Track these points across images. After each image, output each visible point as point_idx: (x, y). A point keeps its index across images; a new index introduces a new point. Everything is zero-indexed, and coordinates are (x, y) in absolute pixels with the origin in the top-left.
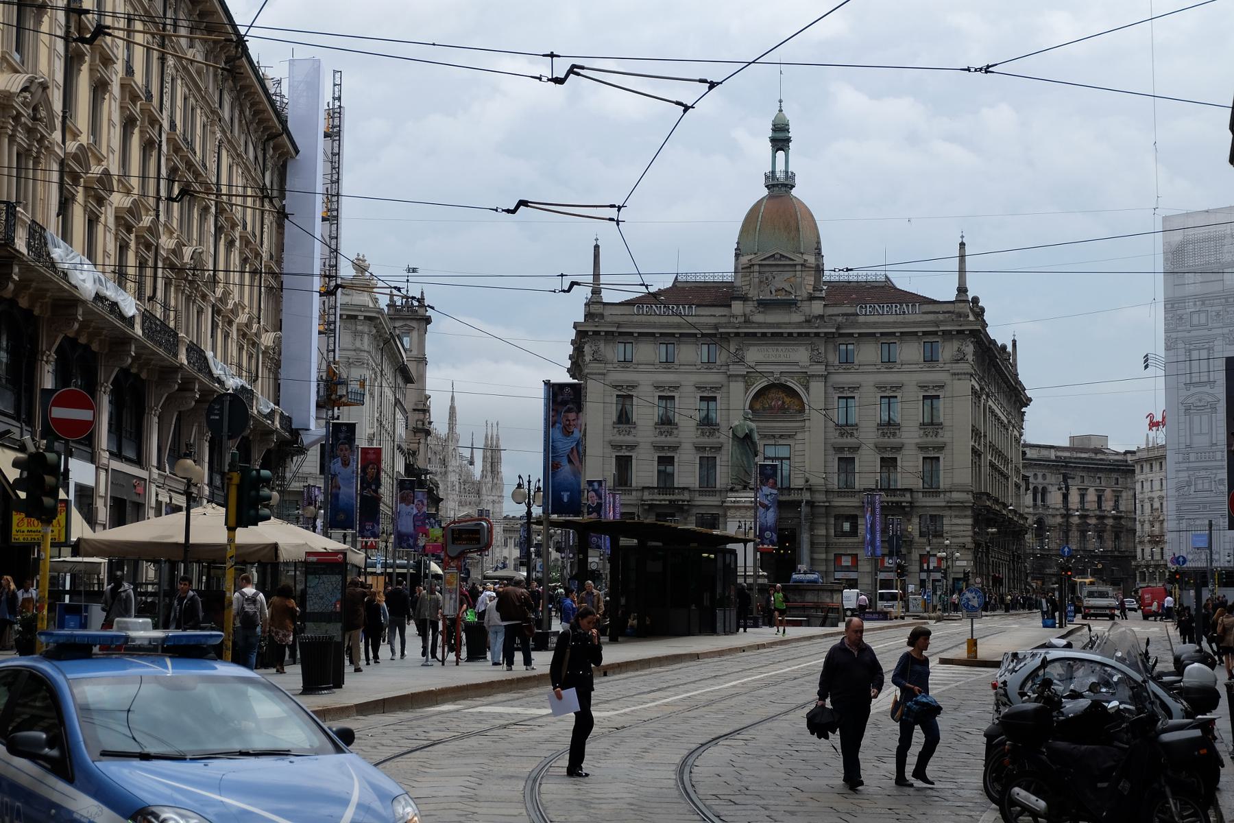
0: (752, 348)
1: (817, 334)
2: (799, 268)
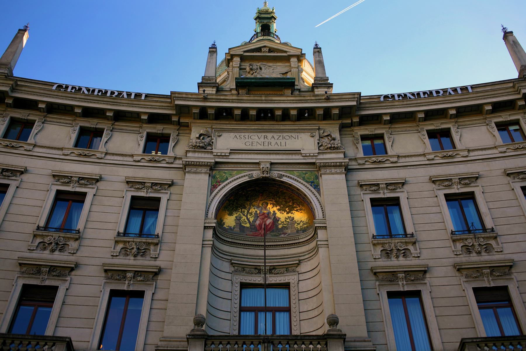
0: (225, 135)
1: (327, 115)
2: (294, 60)
